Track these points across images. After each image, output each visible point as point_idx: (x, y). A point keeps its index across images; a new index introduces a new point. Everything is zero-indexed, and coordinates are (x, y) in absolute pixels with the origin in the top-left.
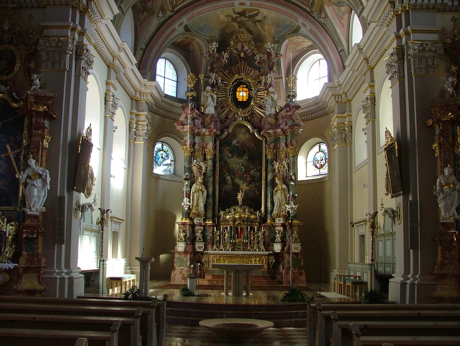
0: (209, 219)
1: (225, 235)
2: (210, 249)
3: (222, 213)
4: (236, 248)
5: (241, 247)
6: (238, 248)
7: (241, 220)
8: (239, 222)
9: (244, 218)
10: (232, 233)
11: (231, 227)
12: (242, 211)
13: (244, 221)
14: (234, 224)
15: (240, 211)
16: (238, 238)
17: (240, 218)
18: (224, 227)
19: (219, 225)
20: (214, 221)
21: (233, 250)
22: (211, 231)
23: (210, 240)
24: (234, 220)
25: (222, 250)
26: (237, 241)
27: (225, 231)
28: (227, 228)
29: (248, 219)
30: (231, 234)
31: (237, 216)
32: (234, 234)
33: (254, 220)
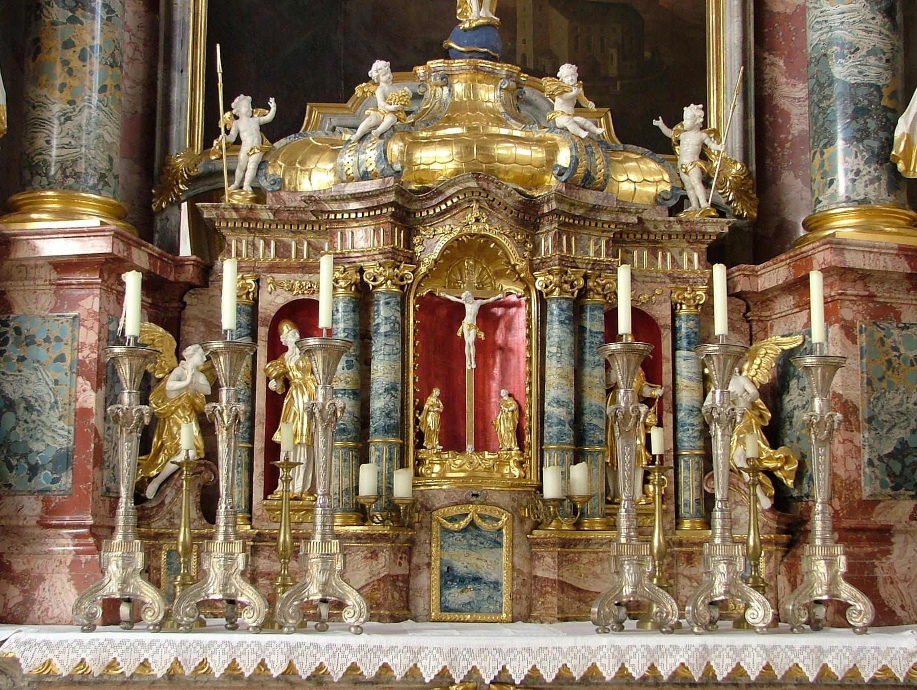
0: (70, 180)
1: (275, 403)
2: (60, 592)
3: (245, 120)
4: (428, 582)
5: (498, 565)
6: (449, 577)
7: (491, 205)
8: (472, 222)
9: (534, 181)
10: (382, 370)
11: (362, 298)
12: (489, 95)
13: (528, 215)
14: (402, 255)
15: (474, 104)
16: (452, 441)
17: (482, 178)
18: (272, 300)
19: (207, 275)
20: (142, 218)
21: (395, 604)
22: (89, 336)
23: (64, 460)
24: (406, 208)
25: (229, 611)
26: (446, 471)
27: (276, 350)
28: (302, 313)
29: (577, 208)
30: (361, 393)
31: (439, 160)
32: (398, 389)
33: (658, 217)
